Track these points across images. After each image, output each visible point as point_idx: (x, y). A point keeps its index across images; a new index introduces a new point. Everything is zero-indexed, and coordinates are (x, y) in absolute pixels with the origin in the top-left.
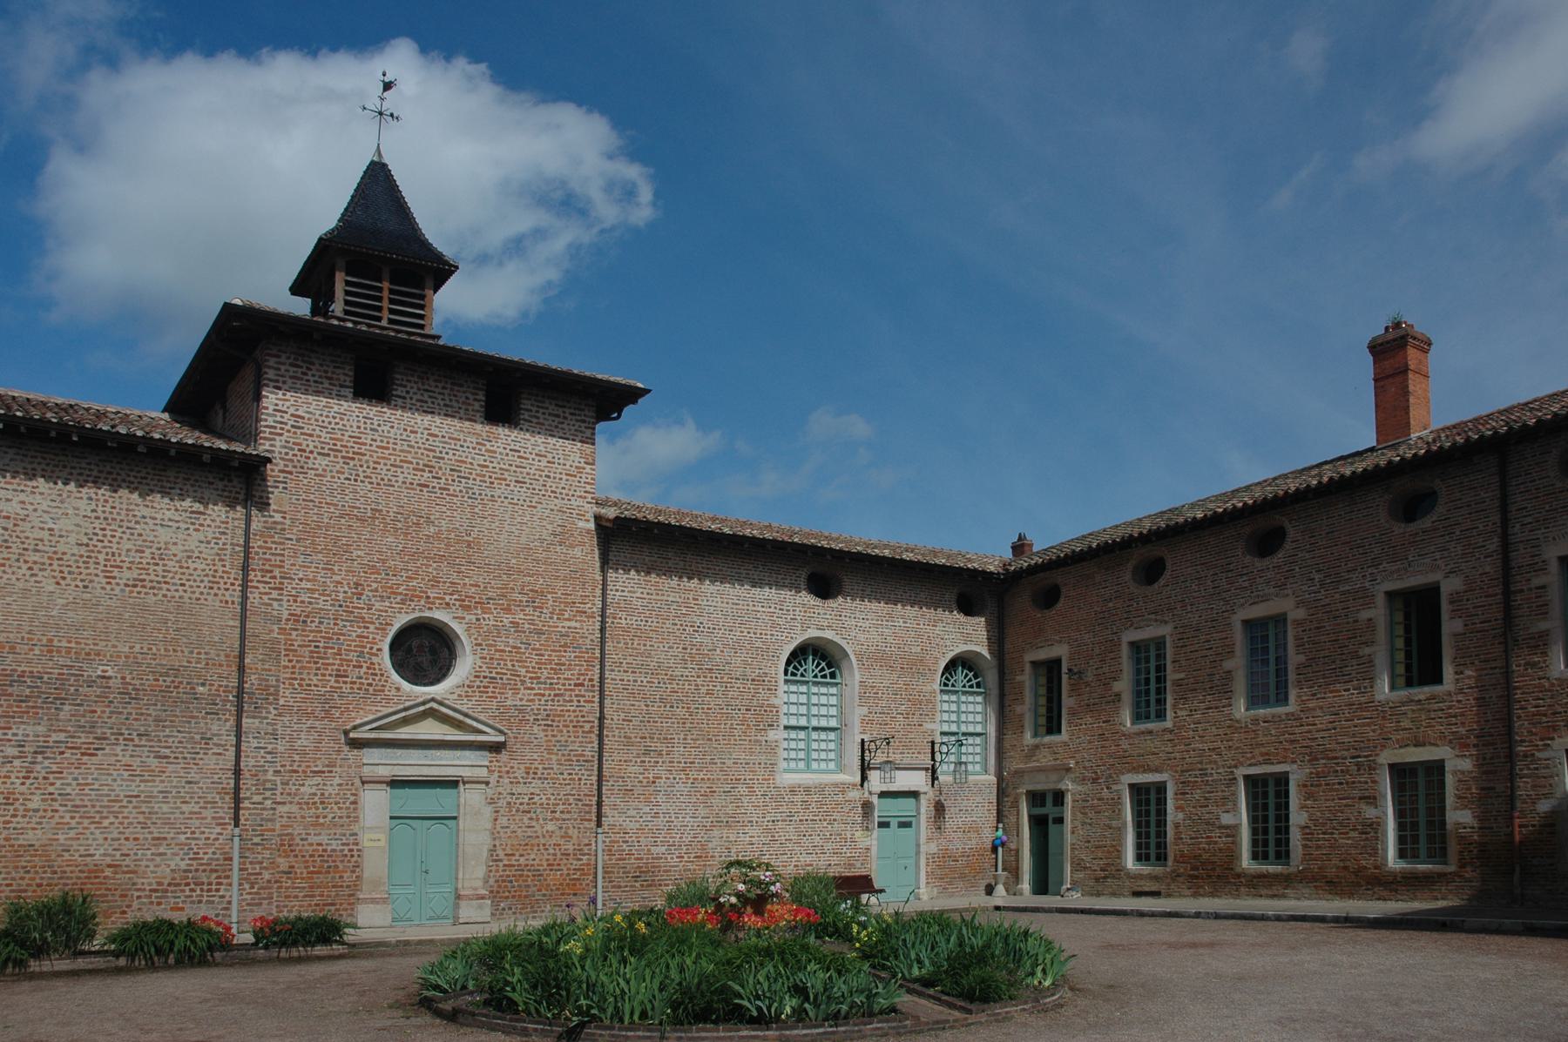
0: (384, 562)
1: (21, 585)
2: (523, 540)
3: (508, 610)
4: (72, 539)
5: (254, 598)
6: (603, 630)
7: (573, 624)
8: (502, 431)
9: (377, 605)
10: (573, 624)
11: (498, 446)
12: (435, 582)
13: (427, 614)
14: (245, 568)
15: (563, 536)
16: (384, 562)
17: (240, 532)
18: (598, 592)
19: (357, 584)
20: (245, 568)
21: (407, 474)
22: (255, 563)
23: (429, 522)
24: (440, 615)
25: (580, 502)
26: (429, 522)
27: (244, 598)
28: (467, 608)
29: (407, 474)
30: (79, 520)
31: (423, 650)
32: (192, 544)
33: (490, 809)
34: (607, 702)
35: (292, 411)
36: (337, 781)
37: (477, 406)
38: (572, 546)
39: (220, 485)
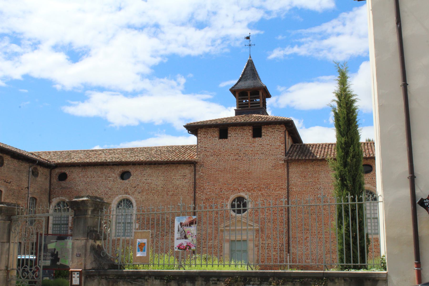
0: (227, 181)
1: (151, 198)
2: (264, 170)
3: (260, 190)
4: (160, 187)
5: (197, 195)
6: (288, 192)
7: (279, 192)
8: (257, 139)
9: (226, 193)
10: (279, 192)
11: (256, 144)
12: (240, 185)
13: (239, 194)
14: (195, 188)
15: (275, 167)
16: (227, 181)
17: (193, 179)
18: (286, 181)
19: (221, 188)
20: (195, 188)
21: (232, 157)
22: (197, 187)
23: (238, 169)
24: (242, 194)
25: (280, 156)
26: (238, 169)
27: (195, 195)
28: (249, 191)
29: (232, 157)
30: (161, 182)
31: (240, 204)
32: (184, 184)
33: (256, 248)
34: (290, 215)
35: (204, 146)
36: (217, 241)
37: (250, 134)
38: (278, 169)
39: (189, 168)
